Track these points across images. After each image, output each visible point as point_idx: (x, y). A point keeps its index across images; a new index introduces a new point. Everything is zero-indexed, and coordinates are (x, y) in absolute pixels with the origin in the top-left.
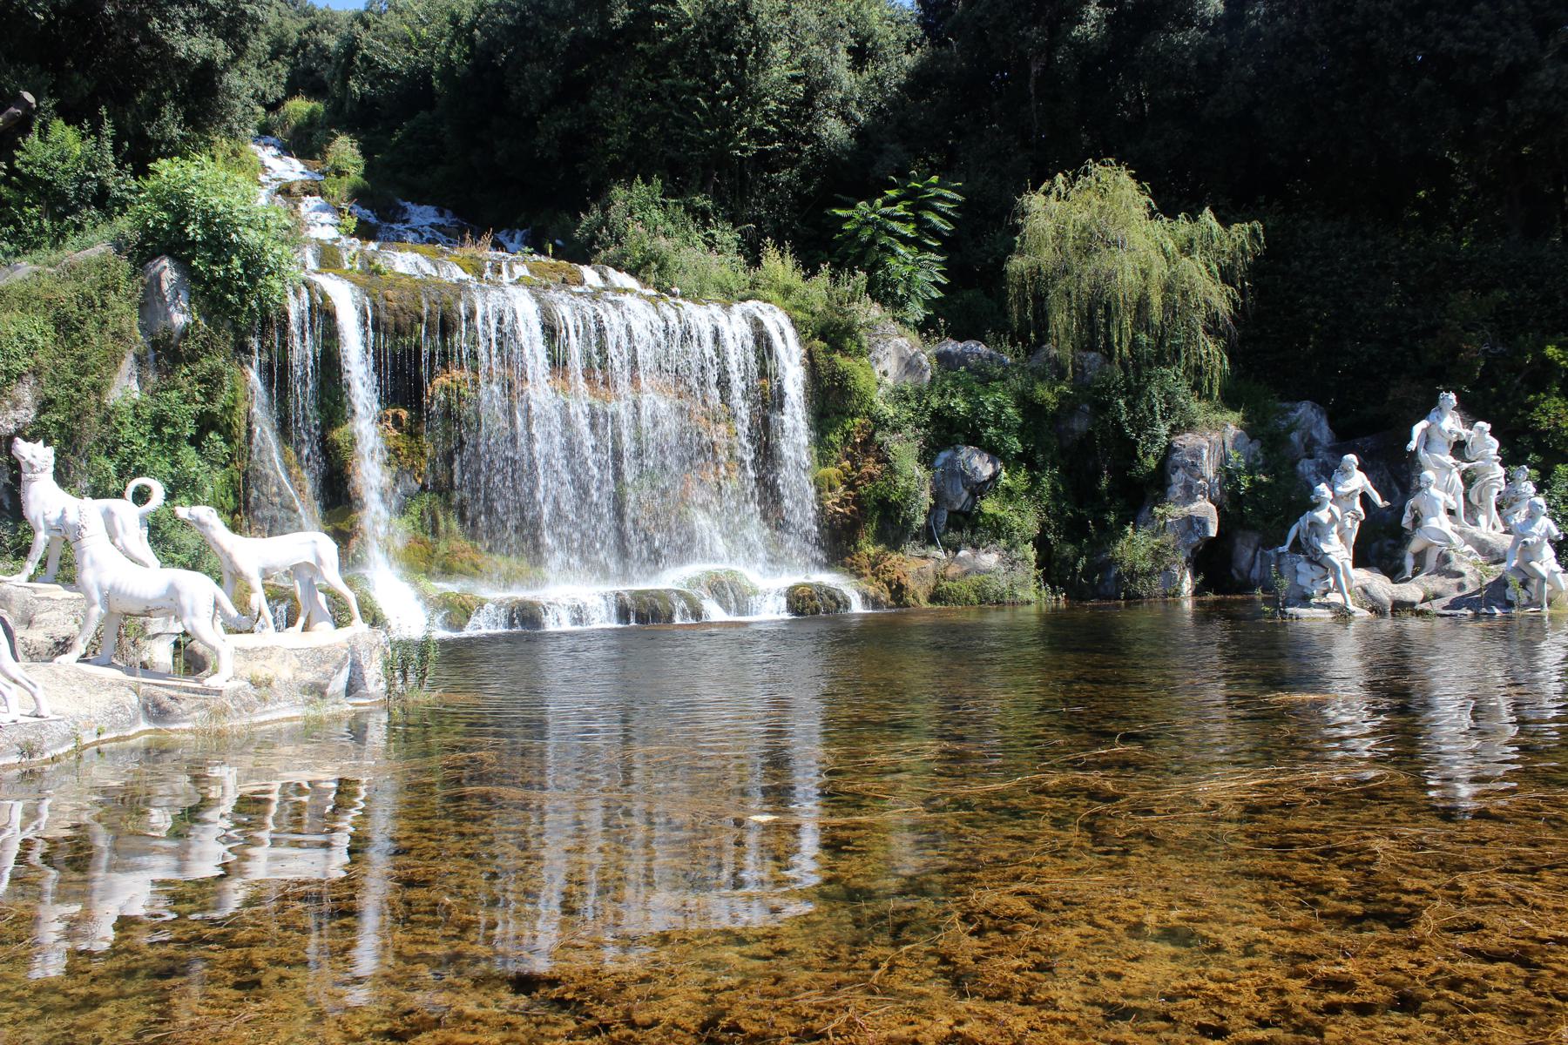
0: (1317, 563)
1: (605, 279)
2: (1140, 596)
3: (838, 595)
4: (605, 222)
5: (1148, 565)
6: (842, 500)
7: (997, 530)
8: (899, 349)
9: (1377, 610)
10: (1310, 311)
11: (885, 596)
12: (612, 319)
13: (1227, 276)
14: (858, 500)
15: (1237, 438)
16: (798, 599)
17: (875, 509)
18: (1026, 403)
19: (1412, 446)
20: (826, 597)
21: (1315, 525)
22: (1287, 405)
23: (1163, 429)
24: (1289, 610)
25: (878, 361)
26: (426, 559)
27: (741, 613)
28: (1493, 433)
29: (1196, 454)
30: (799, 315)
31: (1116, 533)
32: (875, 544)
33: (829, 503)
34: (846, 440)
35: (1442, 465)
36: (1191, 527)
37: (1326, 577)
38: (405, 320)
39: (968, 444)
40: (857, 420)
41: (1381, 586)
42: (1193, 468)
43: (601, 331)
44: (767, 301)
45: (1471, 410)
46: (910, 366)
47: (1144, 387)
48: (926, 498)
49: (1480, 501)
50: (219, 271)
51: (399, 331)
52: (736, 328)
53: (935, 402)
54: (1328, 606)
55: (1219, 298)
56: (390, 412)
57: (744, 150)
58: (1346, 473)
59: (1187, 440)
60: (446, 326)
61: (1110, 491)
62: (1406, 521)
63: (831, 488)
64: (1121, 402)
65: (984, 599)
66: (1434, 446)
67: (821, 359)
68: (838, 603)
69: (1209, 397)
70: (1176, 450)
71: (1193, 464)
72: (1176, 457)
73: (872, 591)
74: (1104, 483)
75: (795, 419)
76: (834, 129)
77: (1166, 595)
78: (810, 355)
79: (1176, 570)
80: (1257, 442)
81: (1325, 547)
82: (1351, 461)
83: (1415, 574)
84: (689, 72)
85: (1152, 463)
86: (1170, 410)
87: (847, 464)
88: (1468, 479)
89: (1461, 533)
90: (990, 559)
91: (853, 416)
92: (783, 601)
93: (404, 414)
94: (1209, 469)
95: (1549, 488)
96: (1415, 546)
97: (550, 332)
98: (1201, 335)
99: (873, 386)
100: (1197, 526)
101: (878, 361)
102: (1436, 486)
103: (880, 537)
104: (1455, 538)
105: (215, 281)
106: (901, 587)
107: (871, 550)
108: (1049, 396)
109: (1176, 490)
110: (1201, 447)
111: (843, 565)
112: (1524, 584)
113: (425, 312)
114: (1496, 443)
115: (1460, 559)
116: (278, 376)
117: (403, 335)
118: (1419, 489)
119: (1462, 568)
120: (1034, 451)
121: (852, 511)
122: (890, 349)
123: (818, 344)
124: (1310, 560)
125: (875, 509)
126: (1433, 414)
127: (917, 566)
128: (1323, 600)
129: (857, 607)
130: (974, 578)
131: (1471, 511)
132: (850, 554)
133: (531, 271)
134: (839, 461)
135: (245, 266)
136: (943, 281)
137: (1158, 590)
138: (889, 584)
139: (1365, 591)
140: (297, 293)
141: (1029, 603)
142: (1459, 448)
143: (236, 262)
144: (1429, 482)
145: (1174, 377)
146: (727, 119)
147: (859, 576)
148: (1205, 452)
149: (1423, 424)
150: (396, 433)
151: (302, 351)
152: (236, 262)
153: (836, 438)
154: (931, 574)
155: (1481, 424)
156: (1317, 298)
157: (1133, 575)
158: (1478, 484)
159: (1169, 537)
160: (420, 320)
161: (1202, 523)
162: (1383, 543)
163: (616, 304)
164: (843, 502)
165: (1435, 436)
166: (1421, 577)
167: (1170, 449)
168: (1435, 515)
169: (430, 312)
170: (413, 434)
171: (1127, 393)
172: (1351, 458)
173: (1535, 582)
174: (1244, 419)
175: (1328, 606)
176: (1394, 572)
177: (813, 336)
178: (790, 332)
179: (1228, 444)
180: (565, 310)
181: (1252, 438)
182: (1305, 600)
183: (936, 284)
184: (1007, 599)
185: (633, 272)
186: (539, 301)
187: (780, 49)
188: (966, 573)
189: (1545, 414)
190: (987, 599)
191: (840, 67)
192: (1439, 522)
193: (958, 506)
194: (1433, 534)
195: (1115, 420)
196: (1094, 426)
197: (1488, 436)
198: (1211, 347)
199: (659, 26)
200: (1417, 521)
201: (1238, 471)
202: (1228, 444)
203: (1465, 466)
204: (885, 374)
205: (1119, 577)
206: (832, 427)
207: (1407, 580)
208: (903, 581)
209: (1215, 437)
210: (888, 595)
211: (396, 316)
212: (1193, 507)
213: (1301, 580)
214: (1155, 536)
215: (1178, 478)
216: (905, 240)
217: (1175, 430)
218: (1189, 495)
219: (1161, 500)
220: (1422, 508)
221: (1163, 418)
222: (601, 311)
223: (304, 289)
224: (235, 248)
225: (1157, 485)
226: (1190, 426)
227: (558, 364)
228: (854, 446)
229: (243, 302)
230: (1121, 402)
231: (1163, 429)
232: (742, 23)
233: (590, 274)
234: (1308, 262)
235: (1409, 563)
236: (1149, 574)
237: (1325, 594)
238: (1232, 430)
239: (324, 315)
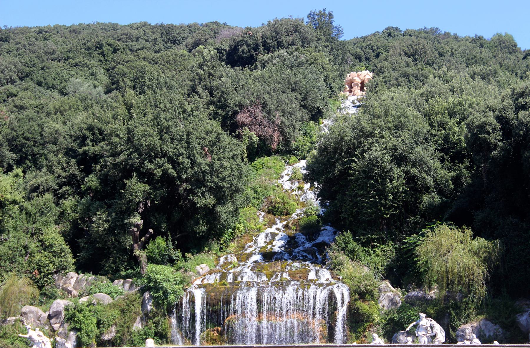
8: (389, 296)
40: (368, 323)
43: (275, 298)
46: (392, 301)
50: (157, 295)
51: (214, 305)
52: (322, 295)
53: (391, 316)
60: (228, 303)
78: (349, 302)
91: (366, 322)
97: (259, 301)
116: (179, 319)
122: (385, 297)
123: (357, 296)
135: (163, 293)
151: (186, 313)
160: (220, 301)
170: (220, 334)
199: (351, 172)
204: (383, 306)
206: (360, 327)
224: (162, 288)
227: (259, 312)
229: (163, 302)
239: (192, 302)
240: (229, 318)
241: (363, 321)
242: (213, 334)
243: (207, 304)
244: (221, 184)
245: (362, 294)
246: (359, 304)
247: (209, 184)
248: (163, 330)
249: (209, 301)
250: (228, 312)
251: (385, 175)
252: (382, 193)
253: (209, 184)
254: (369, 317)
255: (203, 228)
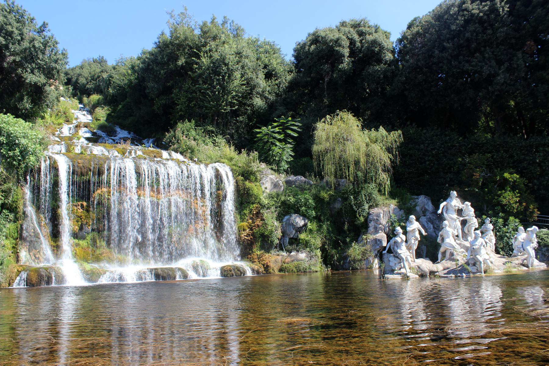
0: (397, 257)
1: (170, 155)
2: (357, 269)
3: (241, 269)
4: (175, 136)
5: (360, 257)
6: (248, 234)
7: (306, 244)
8: (271, 179)
9: (423, 276)
10: (427, 163)
11: (262, 269)
12: (162, 170)
13: (389, 150)
14: (253, 234)
15: (394, 209)
16: (225, 271)
17: (259, 237)
18: (318, 199)
19: (439, 212)
20: (236, 270)
21: (396, 242)
22: (416, 197)
23: (366, 206)
24: (386, 275)
25: (263, 184)
26: (81, 257)
27: (204, 276)
28: (472, 206)
29: (378, 215)
30: (234, 167)
31: (348, 245)
32: (260, 250)
33: (243, 235)
34: (250, 212)
35: (452, 219)
36: (376, 243)
37: (400, 263)
38: (84, 170)
39: (295, 213)
40: (254, 205)
41: (426, 264)
42: (377, 221)
43: (157, 174)
44: (224, 163)
45: (463, 197)
46: (276, 185)
47: (360, 192)
48: (279, 234)
49: (468, 232)
50: (11, 153)
51: (82, 174)
52: (208, 174)
53: (283, 198)
54: (400, 274)
55: (386, 158)
56: (80, 203)
57: (225, 110)
58: (411, 223)
59: (375, 211)
60: (100, 173)
61: (349, 230)
62: (439, 240)
63: (244, 230)
64: (352, 197)
65: (299, 271)
66: (449, 211)
67: (240, 183)
68: (241, 272)
69: (384, 194)
70: (370, 214)
71: (377, 220)
72: (370, 217)
73: (256, 267)
74: (346, 227)
75: (229, 205)
76: (258, 102)
77: (367, 268)
78: (237, 182)
79: (371, 259)
80: (402, 211)
81: (399, 251)
82: (412, 218)
83: (442, 260)
84: (205, 83)
85: (362, 219)
86: (370, 200)
87: (250, 221)
88: (464, 223)
89: (460, 244)
90: (302, 256)
91: (253, 203)
92: (219, 272)
93: (85, 204)
94: (384, 221)
95: (508, 225)
96: (442, 250)
97: (138, 174)
98: (380, 171)
99: (260, 193)
100: (378, 242)
101: (263, 184)
102: (449, 227)
103: (262, 248)
104: (457, 247)
105: (10, 157)
106: (268, 266)
107: (259, 253)
108: (326, 195)
109: (371, 229)
110: (380, 213)
111: (248, 258)
112: (474, 265)
113: (92, 168)
114: (473, 210)
115: (458, 254)
116: (36, 190)
117: (84, 176)
118: (443, 228)
119: (458, 258)
120: (321, 215)
121: (251, 238)
122: (268, 179)
123: (240, 178)
124: (395, 256)
125: (259, 237)
126: (449, 200)
127: (275, 258)
128: (399, 272)
129: (249, 273)
130: (296, 263)
131: (465, 236)
132: (250, 254)
133: (144, 154)
134: (247, 220)
135: (21, 152)
136: (293, 154)
137: (364, 266)
138: (264, 265)
139: (419, 267)
140: (45, 161)
141: (316, 272)
142: (460, 212)
143: (17, 150)
144: (446, 225)
145: (372, 187)
146: (217, 99)
147: (253, 262)
148: (382, 215)
149: (444, 203)
150: (81, 210)
152: (17, 150)
153: (247, 212)
154: (280, 261)
155: (467, 203)
156: (430, 158)
157: (355, 261)
158: (467, 225)
159: (368, 247)
160: (90, 170)
161: (380, 241)
162: (430, 248)
163: (164, 165)
164: (248, 235)
165: (450, 208)
166: (444, 261)
167: (369, 214)
168: (448, 237)
169: (94, 168)
170: (88, 211)
171: (354, 193)
172: (413, 217)
173: (478, 263)
174: (397, 202)
175: (400, 274)
176: (434, 260)
177: (239, 175)
178: (230, 174)
179: (391, 212)
180: (145, 166)
181: (401, 209)
182: (392, 271)
183: (290, 155)
184: (308, 270)
185: (182, 153)
186: (135, 163)
187: (237, 74)
188: (293, 261)
189: (505, 198)
190: (301, 271)
191: (261, 82)
192: (450, 240)
193: (292, 236)
194: (447, 245)
195: (350, 204)
196: (343, 206)
197: (470, 207)
198: (384, 176)
200: (443, 240)
201: (395, 221)
202: (391, 212)
203: (462, 219)
204: (266, 188)
205: (350, 262)
206: (245, 208)
207: (439, 263)
208: (269, 264)
209: (385, 209)
210: (263, 269)
211: (81, 169)
212: (377, 235)
213: (392, 264)
214: (363, 246)
215: (372, 225)
216: (280, 140)
217: (370, 207)
218: (376, 231)
219: (366, 233)
220: (444, 235)
221: (367, 203)
222: (158, 167)
223: (48, 160)
224: (18, 145)
225: (365, 226)
226: (377, 205)
227: (140, 186)
228: (253, 215)
229: (19, 164)
230: (352, 197)
231: (366, 206)
232: (223, 66)
233: (165, 154)
234: (426, 145)
235: (440, 256)
236: (361, 260)
237: (400, 269)
238: (393, 206)
239: (54, 168)
240: (99, 191)
241: (249, 202)
242: (77, 210)
243: (73, 173)
244: (53, 65)
245: (246, 174)
246: (247, 183)
247: (39, 61)
248: (13, 202)
249: (76, 169)
250: (99, 184)
251: (230, 73)
252: (225, 90)
253: (39, 61)
254: (256, 199)
255: (28, 106)
